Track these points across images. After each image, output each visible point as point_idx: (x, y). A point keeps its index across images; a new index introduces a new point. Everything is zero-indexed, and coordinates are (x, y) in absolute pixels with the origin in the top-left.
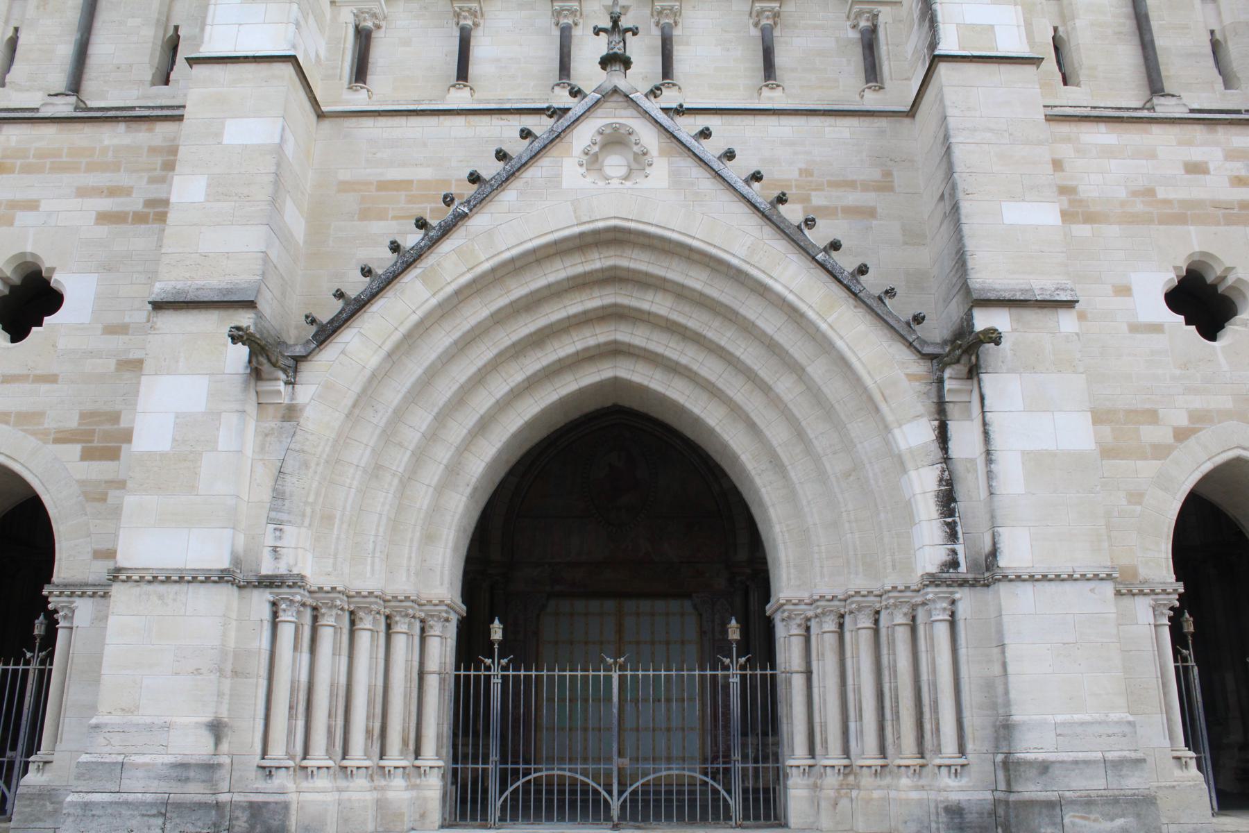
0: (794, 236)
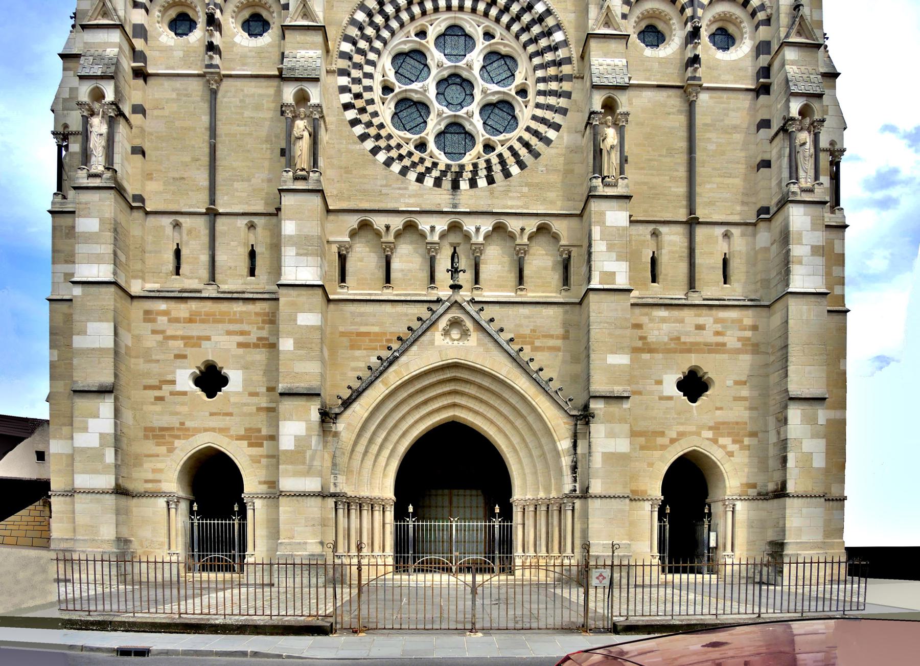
0: (523, 367)
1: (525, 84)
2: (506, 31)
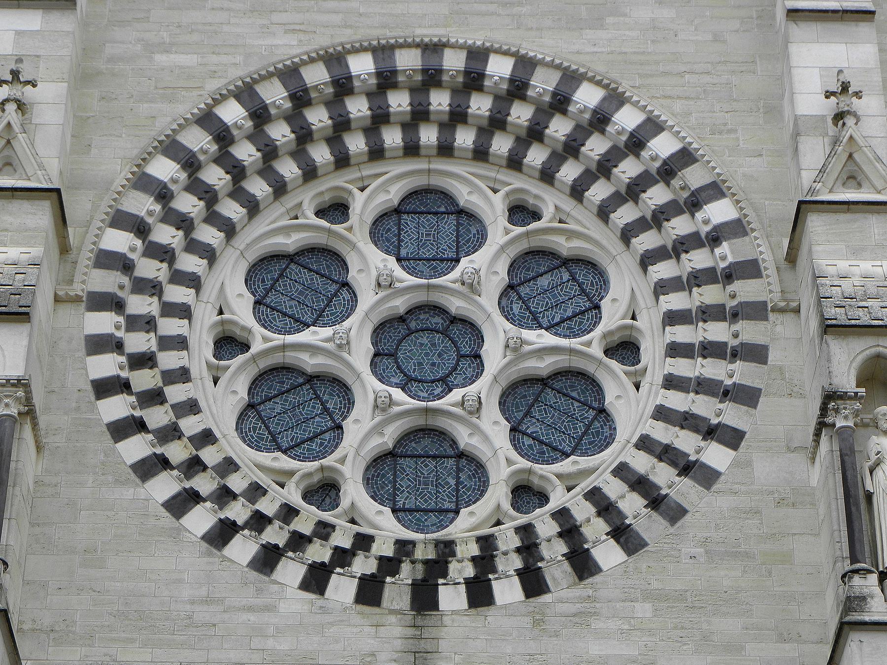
1: (631, 327)
2: (573, 202)
